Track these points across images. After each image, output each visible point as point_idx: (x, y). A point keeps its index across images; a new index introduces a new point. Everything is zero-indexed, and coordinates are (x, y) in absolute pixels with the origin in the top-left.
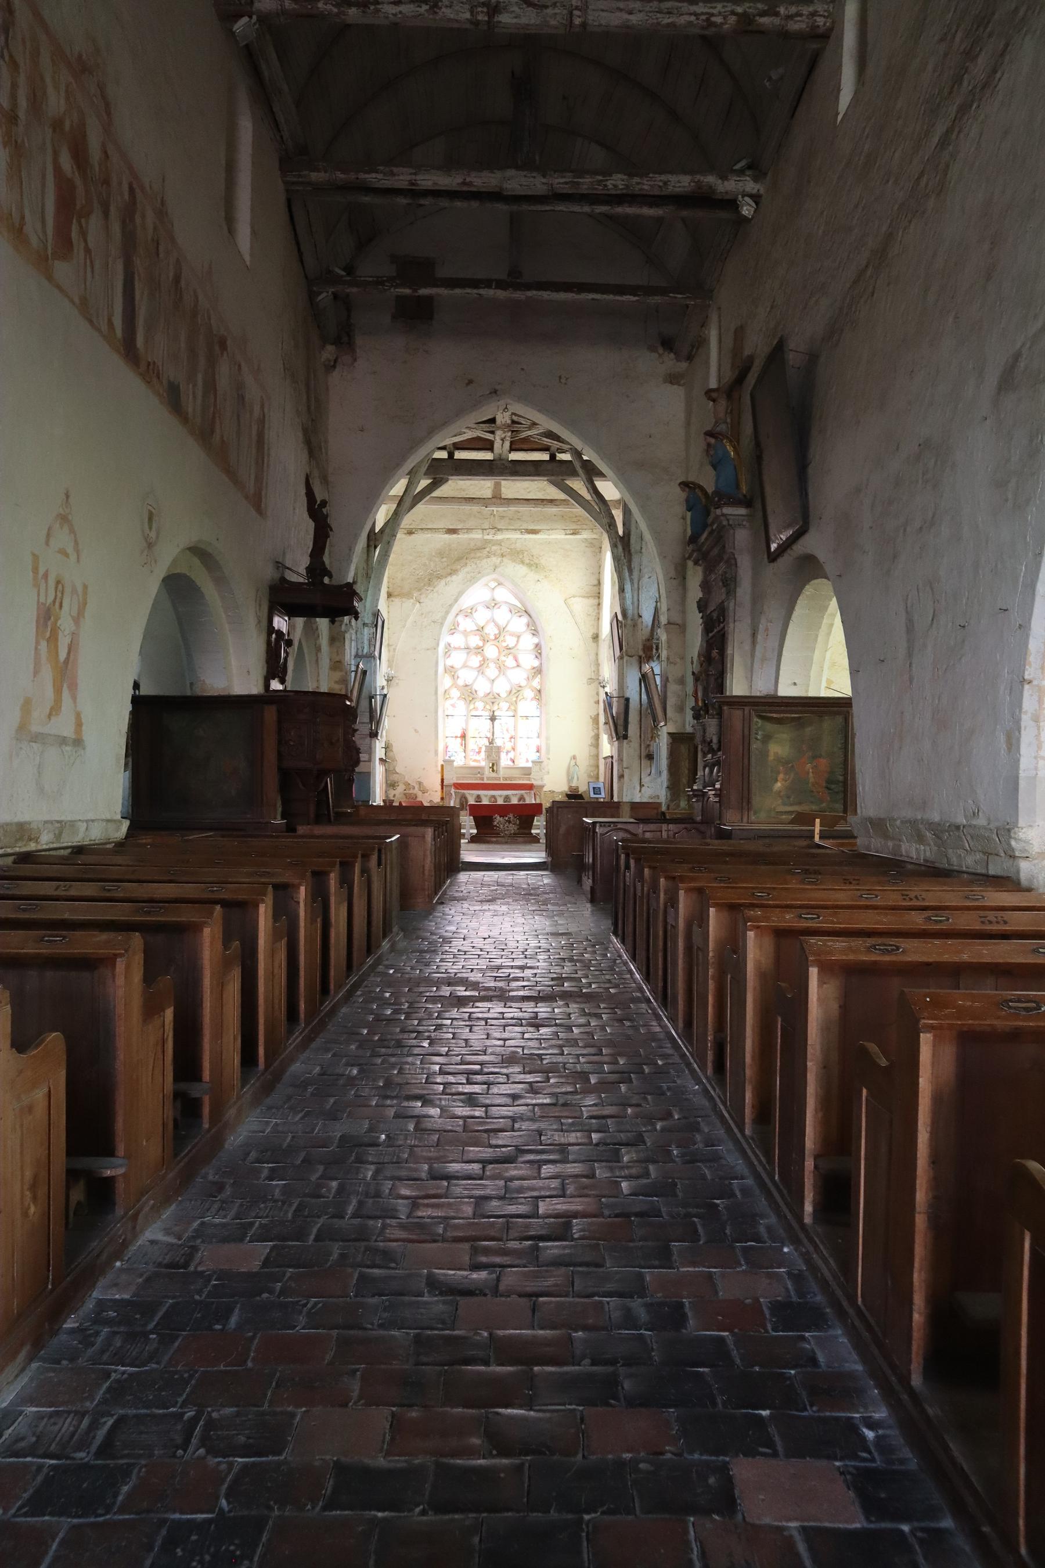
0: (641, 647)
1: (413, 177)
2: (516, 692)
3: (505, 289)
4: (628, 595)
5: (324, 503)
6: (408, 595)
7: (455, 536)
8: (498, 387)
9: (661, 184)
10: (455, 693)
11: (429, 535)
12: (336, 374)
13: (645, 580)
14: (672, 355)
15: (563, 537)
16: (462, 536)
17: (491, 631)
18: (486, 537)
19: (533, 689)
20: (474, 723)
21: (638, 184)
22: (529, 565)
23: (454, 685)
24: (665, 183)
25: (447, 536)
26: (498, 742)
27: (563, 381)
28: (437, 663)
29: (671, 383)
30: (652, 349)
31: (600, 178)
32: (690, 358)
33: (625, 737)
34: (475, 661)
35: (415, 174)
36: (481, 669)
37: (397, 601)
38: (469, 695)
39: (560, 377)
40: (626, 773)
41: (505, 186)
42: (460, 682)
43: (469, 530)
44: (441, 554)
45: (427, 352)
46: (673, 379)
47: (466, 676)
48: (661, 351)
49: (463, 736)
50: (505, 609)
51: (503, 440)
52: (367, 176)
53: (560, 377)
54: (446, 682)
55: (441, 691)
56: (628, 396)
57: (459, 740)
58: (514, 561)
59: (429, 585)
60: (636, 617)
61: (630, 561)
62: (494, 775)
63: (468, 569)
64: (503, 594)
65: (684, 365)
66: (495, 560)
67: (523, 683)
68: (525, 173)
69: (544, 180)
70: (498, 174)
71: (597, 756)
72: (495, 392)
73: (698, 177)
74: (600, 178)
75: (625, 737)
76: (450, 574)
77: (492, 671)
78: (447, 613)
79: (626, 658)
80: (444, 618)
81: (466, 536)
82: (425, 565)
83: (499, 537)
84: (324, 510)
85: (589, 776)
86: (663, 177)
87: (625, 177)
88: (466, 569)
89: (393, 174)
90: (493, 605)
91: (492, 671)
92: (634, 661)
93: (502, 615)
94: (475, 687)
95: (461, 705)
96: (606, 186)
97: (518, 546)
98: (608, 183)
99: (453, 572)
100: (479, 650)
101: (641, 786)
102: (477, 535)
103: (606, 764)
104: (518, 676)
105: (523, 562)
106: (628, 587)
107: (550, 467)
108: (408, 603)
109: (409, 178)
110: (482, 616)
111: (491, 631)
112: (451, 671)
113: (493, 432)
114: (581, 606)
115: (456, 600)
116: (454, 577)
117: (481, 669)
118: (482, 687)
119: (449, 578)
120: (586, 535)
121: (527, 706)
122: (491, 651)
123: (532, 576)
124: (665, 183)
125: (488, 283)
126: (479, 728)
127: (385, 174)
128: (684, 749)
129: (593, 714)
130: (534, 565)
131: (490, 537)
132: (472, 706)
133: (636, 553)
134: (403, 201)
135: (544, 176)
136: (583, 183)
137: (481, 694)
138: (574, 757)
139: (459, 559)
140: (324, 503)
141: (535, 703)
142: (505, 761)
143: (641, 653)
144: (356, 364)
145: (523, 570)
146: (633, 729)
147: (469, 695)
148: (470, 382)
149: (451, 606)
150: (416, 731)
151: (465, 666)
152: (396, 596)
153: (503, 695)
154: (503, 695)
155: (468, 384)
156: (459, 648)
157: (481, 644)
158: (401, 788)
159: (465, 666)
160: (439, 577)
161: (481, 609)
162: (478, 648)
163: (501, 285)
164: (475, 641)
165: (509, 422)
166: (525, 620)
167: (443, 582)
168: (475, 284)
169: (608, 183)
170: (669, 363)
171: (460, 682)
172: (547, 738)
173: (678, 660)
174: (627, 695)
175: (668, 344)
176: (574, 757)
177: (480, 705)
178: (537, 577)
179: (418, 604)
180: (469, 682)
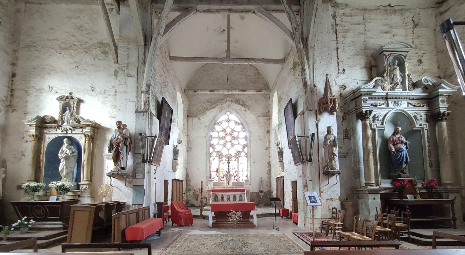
0: (316, 104)
2: (238, 155)
4: (307, 72)
6: (196, 116)
7: (213, 93)
10: (214, 154)
17: (228, 130)
19: (244, 152)
20: (221, 165)
22: (242, 105)
23: (214, 151)
25: (210, 93)
26: (231, 173)
34: (222, 142)
36: (224, 145)
38: (220, 155)
42: (216, 150)
44: (208, 101)
47: (218, 148)
49: (217, 171)
50: (233, 122)
54: (211, 150)
57: (216, 172)
58: (236, 103)
59: (204, 113)
60: (313, 86)
61: (307, 54)
64: (233, 117)
67: (241, 150)
76: (212, 109)
77: (229, 145)
81: (217, 93)
90: (228, 121)
91: (229, 145)
93: (232, 125)
94: (222, 152)
95: (217, 159)
97: (238, 97)
99: (213, 108)
100: (223, 138)
102: (221, 92)
104: (239, 148)
110: (224, 125)
111: (228, 130)
112: (211, 145)
116: (213, 110)
117: (224, 145)
118: (225, 152)
119: (211, 110)
120: (263, 92)
121: (243, 159)
122: (228, 138)
123: (243, 109)
126: (224, 167)
132: (221, 159)
137: (224, 155)
139: (215, 103)
141: (245, 158)
142: (233, 180)
143: (317, 108)
147: (220, 155)
150: (198, 169)
151: (218, 144)
153: (233, 155)
154: (233, 155)
156: (216, 138)
159: (218, 144)
160: (208, 110)
161: (224, 122)
162: (223, 137)
164: (222, 134)
166: (241, 126)
167: (209, 111)
171: (216, 150)
172: (250, 171)
176: (261, 178)
177: (224, 159)
178: (245, 109)
180: (220, 150)
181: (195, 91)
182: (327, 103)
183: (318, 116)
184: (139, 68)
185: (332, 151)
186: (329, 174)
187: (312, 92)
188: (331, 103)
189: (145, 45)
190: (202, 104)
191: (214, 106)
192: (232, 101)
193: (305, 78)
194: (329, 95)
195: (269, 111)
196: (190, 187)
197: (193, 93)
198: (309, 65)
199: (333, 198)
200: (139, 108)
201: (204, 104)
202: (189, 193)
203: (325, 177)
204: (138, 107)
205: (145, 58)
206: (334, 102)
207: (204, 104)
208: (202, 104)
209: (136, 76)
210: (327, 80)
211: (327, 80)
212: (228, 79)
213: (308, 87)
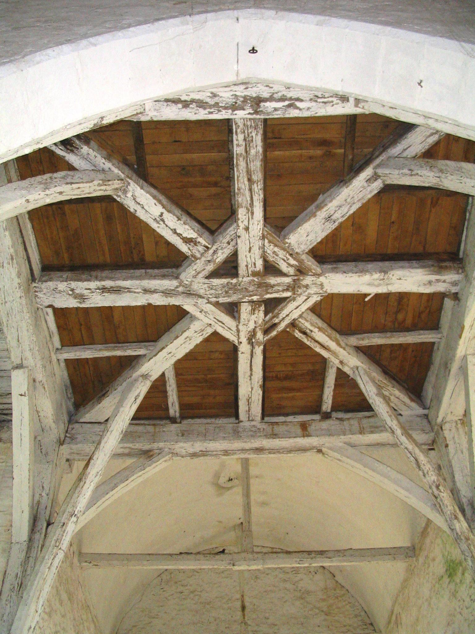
113: (232, 309)
165: (260, 265)
212: (243, 608)
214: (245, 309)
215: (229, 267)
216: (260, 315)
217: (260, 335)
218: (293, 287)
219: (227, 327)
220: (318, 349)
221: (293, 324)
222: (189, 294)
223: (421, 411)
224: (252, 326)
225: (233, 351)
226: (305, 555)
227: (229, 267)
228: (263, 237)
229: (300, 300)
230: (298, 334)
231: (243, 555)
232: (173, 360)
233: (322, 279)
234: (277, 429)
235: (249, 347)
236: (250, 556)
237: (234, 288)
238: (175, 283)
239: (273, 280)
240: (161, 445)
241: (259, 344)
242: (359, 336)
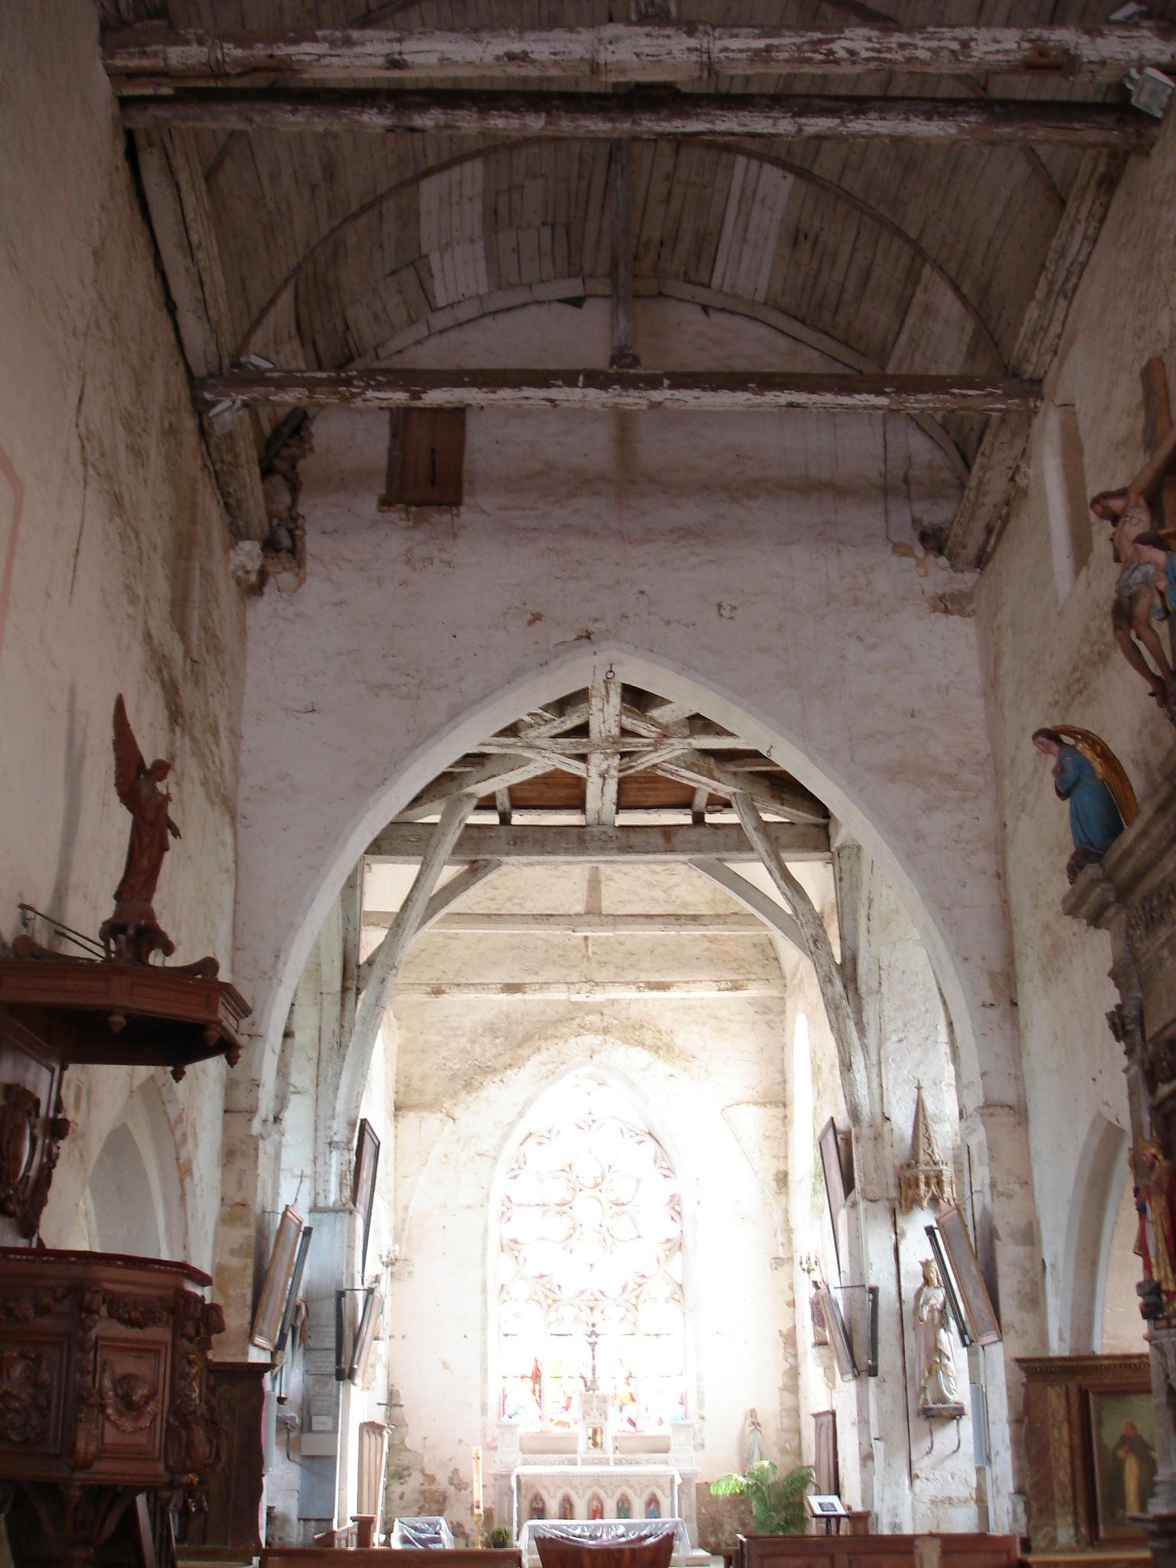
0: (892, 1181)
1: (396, 47)
3: (604, 386)
5: (161, 769)
6: (432, 1106)
7: (518, 996)
8: (592, 627)
9: (955, 46)
11: (471, 996)
12: (261, 610)
13: (891, 1045)
14: (943, 561)
15: (715, 994)
16: (531, 997)
18: (575, 998)
21: (902, 46)
22: (655, 1049)
24: (965, 44)
25: (503, 996)
26: (604, 1387)
27: (726, 613)
28: (486, 1231)
29: (946, 611)
30: (901, 550)
31: (817, 35)
32: (981, 561)
33: (873, 1371)
35: (400, 41)
37: (411, 1118)
39: (720, 606)
40: (879, 1448)
41: (603, 57)
43: (545, 985)
44: (492, 1030)
45: (449, 564)
46: (947, 604)
48: (919, 551)
51: (603, 776)
52: (292, 50)
53: (720, 606)
55: (493, 1286)
56: (860, 639)
57: (529, 1383)
60: (879, 1119)
61: (859, 1011)
62: (596, 1454)
63: (543, 1055)
65: (968, 579)
66: (591, 1040)
68: (649, 29)
69: (693, 43)
70: (587, 36)
71: (795, 1412)
72: (588, 636)
73: (1036, 32)
74: (817, 35)
75: (873, 1371)
78: (505, 1137)
79: (862, 1205)
80: (500, 1147)
81: (538, 996)
82: (464, 1051)
83: (599, 996)
84: (160, 786)
85: (783, 1451)
86: (959, 33)
87: (874, 33)
88: (537, 1058)
89: (349, 42)
92: (882, 1210)
96: (831, 52)
97: (635, 1012)
98: (836, 46)
101: (912, 1477)
102: (558, 994)
103: (819, 1428)
105: (641, 1043)
106: (858, 1061)
107: (694, 835)
108: (433, 1121)
109: (386, 48)
113: (583, 758)
114: (753, 1120)
115: (521, 1115)
119: (509, 1072)
120: (754, 991)
123: (661, 1067)
124: (965, 44)
125: (569, 378)
127: (332, 44)
128: (1054, 1397)
129: (785, 1327)
130: (662, 1048)
131: (580, 998)
133: (870, 992)
134: (374, 120)
135: (690, 34)
136: (778, 48)
138: (753, 1413)
139: (528, 1038)
140: (161, 769)
143: (893, 1193)
144: (304, 588)
145: (640, 1057)
146: (888, 1357)
147: (548, 1295)
148: (537, 617)
149: (511, 1125)
150: (445, 1365)
152: (410, 1108)
155: (530, 623)
157: (568, 1196)
158: (415, 1482)
160: (487, 1070)
163: (595, 379)
164: (558, 1191)
165: (616, 731)
168: (542, 379)
169: (836, 46)
170: (939, 575)
172: (699, 1378)
173: (1016, 1187)
174: (872, 1281)
175: (934, 540)
176: (753, 1413)
179: (450, 1122)
181: (437, 992)
182: (917, 1186)
183: (899, 1219)
184: (323, 1064)
185: (936, 1340)
186: (938, 1414)
187: (877, 1137)
188: (928, 1184)
189: (344, 989)
190: (463, 1042)
191: (525, 1051)
192: (606, 1031)
193: (852, 1094)
194: (923, 1157)
195: (785, 1081)
196: (405, 1459)
197: (426, 998)
198: (865, 1048)
199: (953, 1495)
200: (322, 1196)
201: (473, 1042)
202: (397, 1488)
203: (925, 1425)
204: (317, 1194)
205: (341, 1035)
206: (939, 1183)
207: (473, 1042)
208: (463, 1042)
209: (312, 1089)
210: (920, 1105)
211: (920, 1105)
213: (865, 1125)
214: (596, 759)
215: (582, 730)
216: (616, 761)
217: (614, 773)
218: (656, 746)
219: (576, 768)
220: (685, 782)
221: (654, 766)
222: (530, 747)
223: (821, 821)
224: (604, 767)
225: (579, 783)
226: (672, 919)
227: (582, 730)
228: (621, 714)
229: (661, 752)
230: (660, 773)
231: (589, 918)
232: (507, 784)
233: (689, 740)
234: (635, 839)
235: (600, 780)
236: (596, 920)
237: (585, 745)
238: (512, 740)
239: (630, 740)
240: (488, 857)
241: (612, 777)
242: (739, 762)
